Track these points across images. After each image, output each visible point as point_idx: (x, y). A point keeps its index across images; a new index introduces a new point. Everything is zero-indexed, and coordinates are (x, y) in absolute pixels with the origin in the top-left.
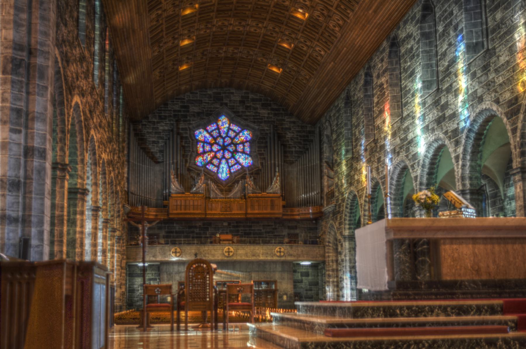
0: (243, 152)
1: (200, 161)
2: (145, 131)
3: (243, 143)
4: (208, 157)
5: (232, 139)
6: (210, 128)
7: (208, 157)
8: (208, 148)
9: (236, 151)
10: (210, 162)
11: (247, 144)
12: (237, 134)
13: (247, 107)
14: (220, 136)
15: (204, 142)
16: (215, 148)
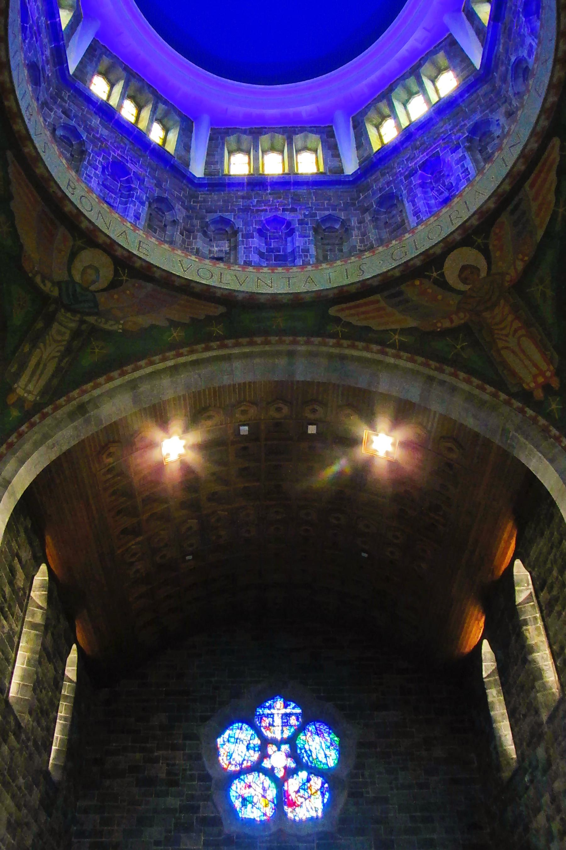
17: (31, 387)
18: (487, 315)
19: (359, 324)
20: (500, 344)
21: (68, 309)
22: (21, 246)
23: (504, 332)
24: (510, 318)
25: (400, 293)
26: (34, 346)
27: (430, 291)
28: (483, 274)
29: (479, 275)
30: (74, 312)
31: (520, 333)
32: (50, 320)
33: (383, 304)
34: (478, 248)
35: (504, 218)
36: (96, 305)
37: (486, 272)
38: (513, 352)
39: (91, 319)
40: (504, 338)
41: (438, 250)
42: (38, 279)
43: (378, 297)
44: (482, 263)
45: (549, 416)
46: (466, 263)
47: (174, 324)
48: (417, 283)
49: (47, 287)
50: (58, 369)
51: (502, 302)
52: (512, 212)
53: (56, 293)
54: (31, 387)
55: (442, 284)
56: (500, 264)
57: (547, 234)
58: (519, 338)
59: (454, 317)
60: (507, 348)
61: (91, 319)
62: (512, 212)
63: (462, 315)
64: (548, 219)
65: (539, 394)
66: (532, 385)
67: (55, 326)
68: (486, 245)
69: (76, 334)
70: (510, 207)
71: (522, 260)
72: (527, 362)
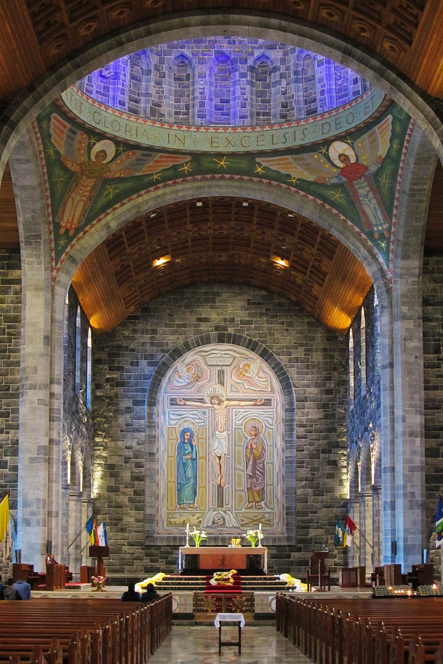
18: (84, 178)
19: (51, 131)
20: (73, 195)
23: (81, 192)
24: (88, 189)
25: (74, 133)
27: (83, 145)
28: (104, 162)
29: (103, 160)
31: (84, 198)
33: (66, 130)
34: (117, 150)
35: (139, 153)
37: (107, 162)
38: (73, 202)
40: (77, 193)
41: (108, 135)
43: (68, 125)
44: (109, 158)
45: (57, 245)
46: (106, 150)
48: (85, 136)
51: (95, 179)
52: (143, 155)
55: (90, 148)
56: (114, 166)
57: (139, 177)
58: (81, 200)
59: (75, 165)
60: (73, 199)
62: (143, 155)
63: (78, 167)
64: (147, 173)
65: (62, 231)
66: (64, 225)
68: (121, 153)
70: (146, 152)
71: (121, 174)
72: (72, 213)
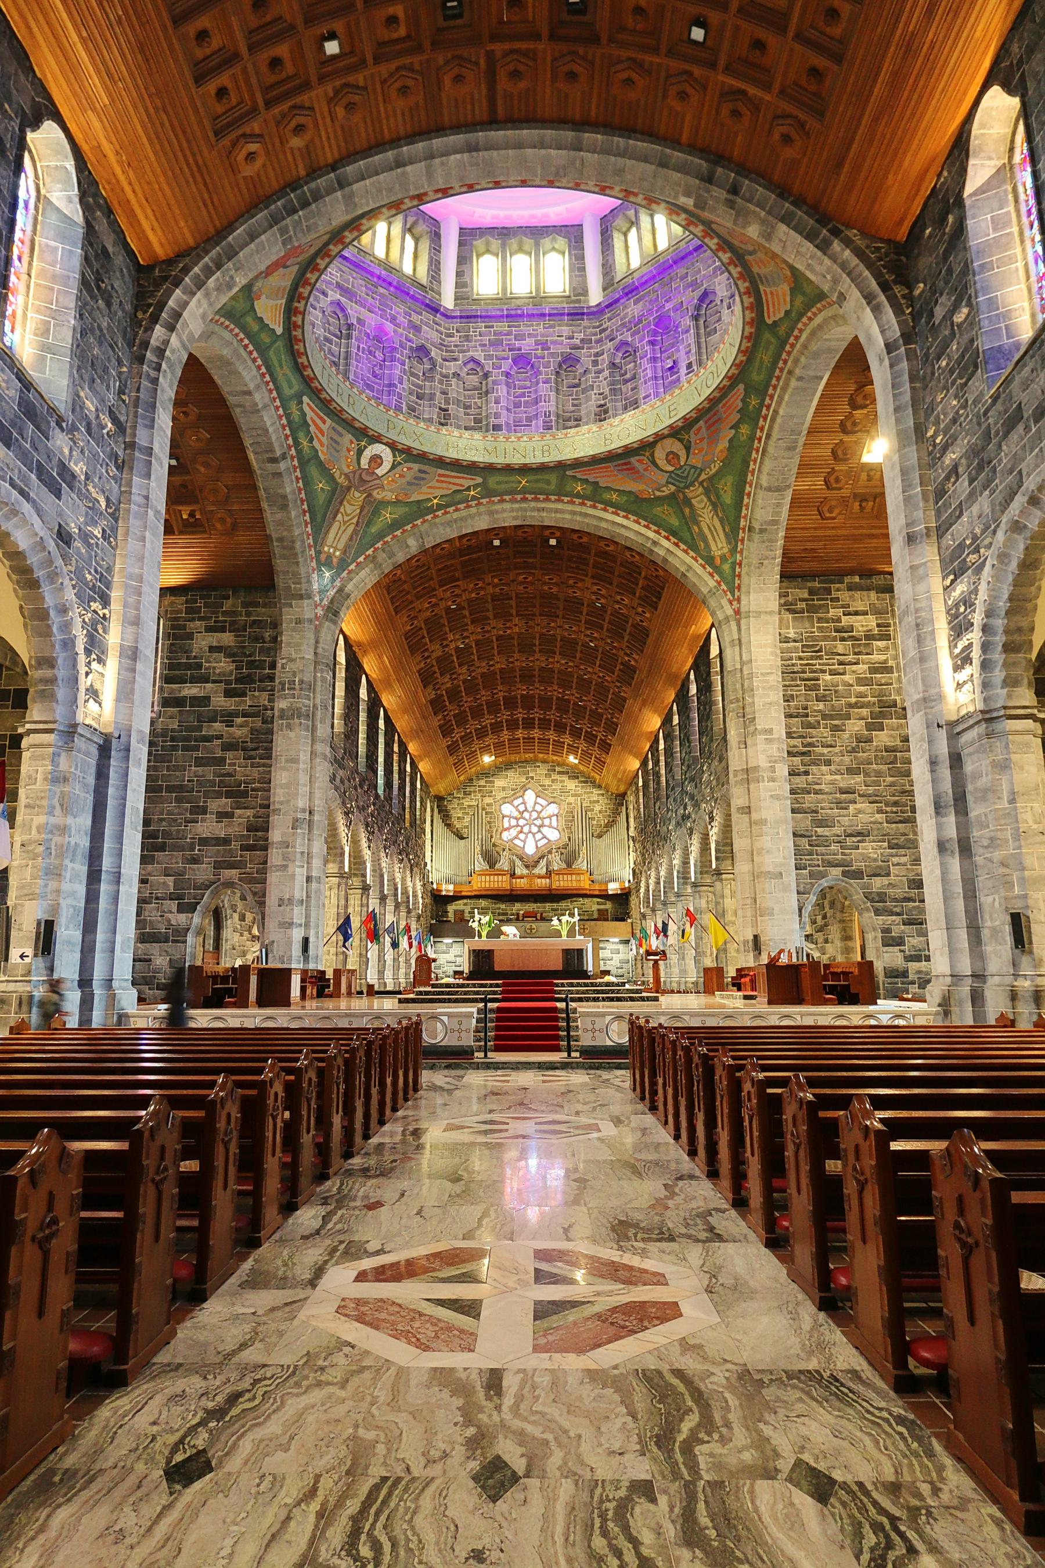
0: (550, 826)
1: (506, 836)
2: (449, 807)
3: (550, 817)
4: (513, 832)
5: (539, 813)
6: (516, 803)
7: (513, 832)
8: (514, 822)
9: (542, 826)
10: (516, 837)
11: (554, 819)
12: (544, 808)
13: (553, 781)
14: (526, 810)
15: (510, 817)
16: (522, 822)
17: (720, 545)
21: (688, 487)
22: (630, 492)
26: (698, 524)
30: (692, 484)
32: (688, 502)
36: (696, 468)
39: (703, 477)
42: (658, 494)
47: (735, 427)
49: (667, 491)
50: (721, 520)
53: (673, 488)
54: (720, 545)
61: (703, 477)
67: (693, 501)
69: (707, 492)
